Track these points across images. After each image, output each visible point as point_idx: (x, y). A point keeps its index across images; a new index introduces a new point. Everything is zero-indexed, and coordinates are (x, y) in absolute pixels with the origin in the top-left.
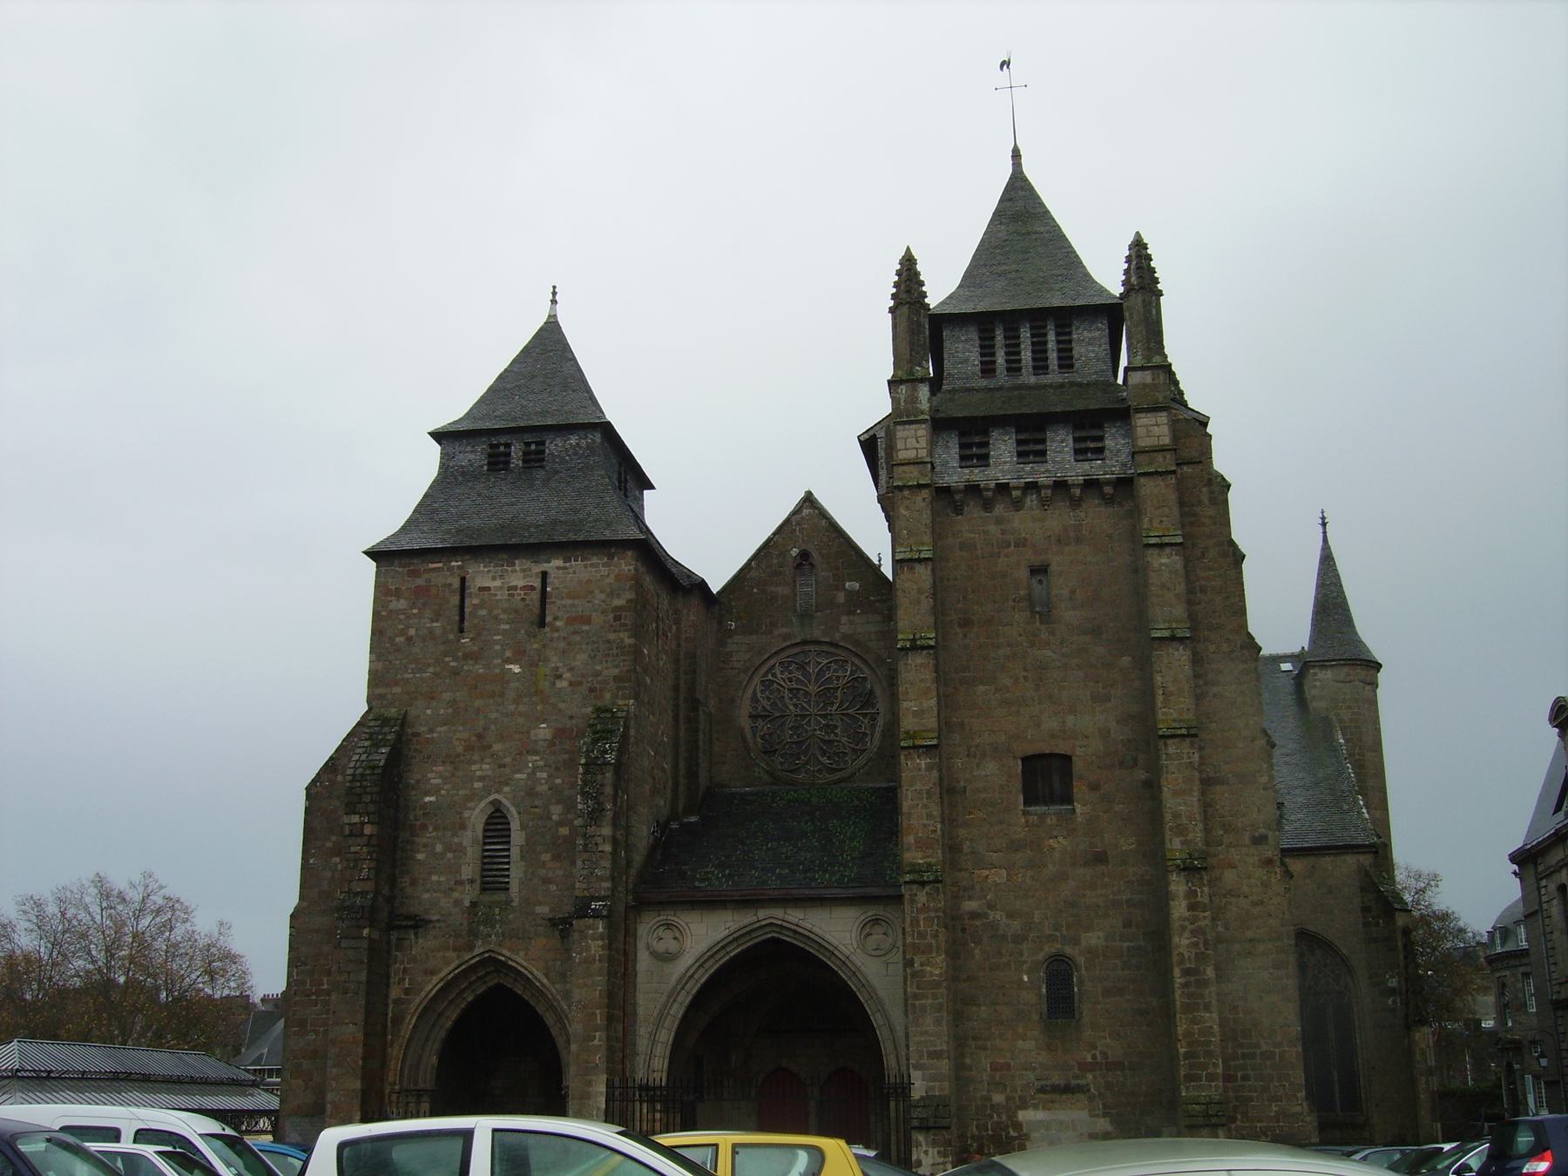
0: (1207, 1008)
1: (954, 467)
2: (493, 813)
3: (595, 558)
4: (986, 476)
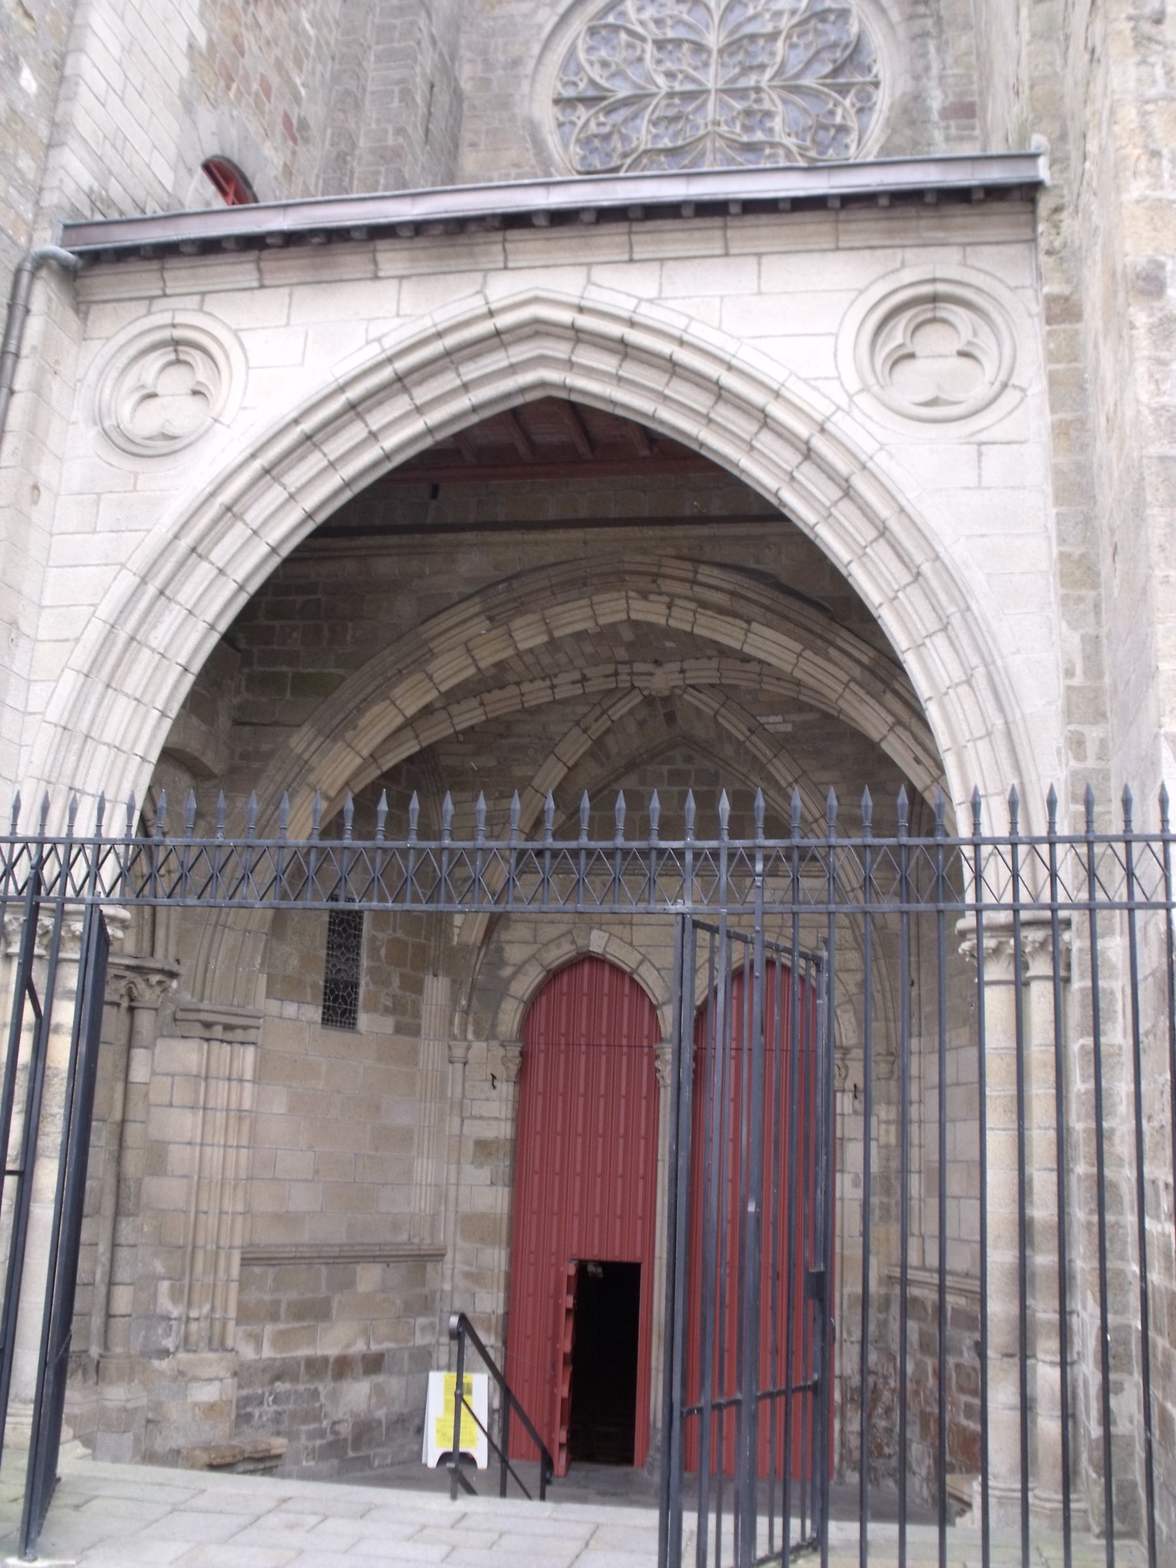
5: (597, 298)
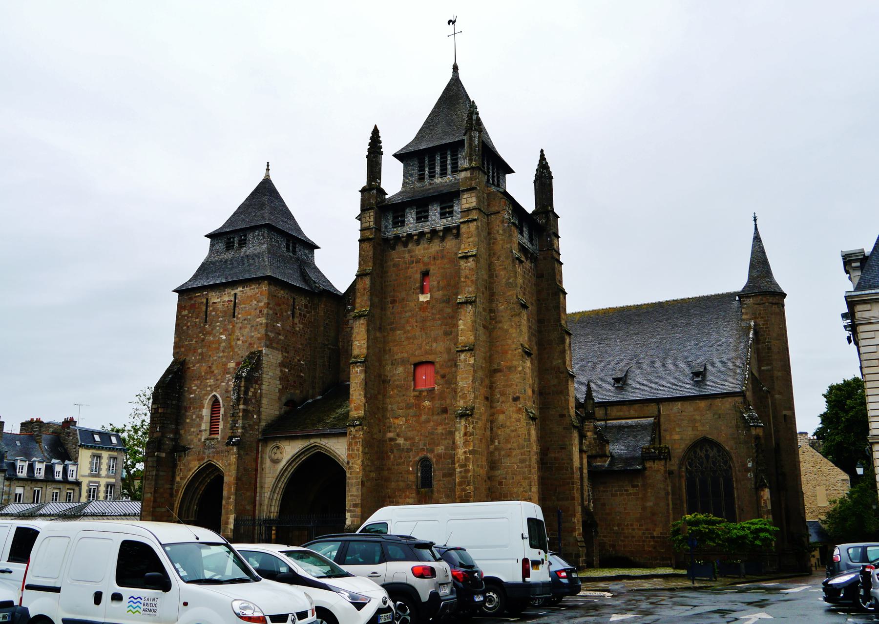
0: (469, 485)
1: (390, 228)
2: (215, 401)
4: (403, 231)
5: (322, 442)
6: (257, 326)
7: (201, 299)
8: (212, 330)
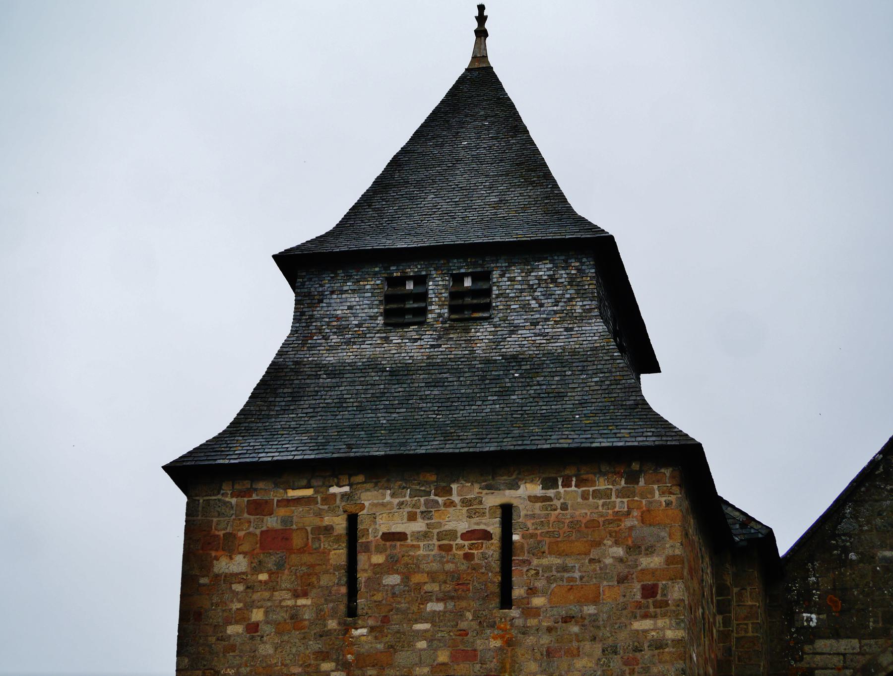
3: (601, 480)
6: (637, 650)
7: (319, 514)
8: (392, 648)
